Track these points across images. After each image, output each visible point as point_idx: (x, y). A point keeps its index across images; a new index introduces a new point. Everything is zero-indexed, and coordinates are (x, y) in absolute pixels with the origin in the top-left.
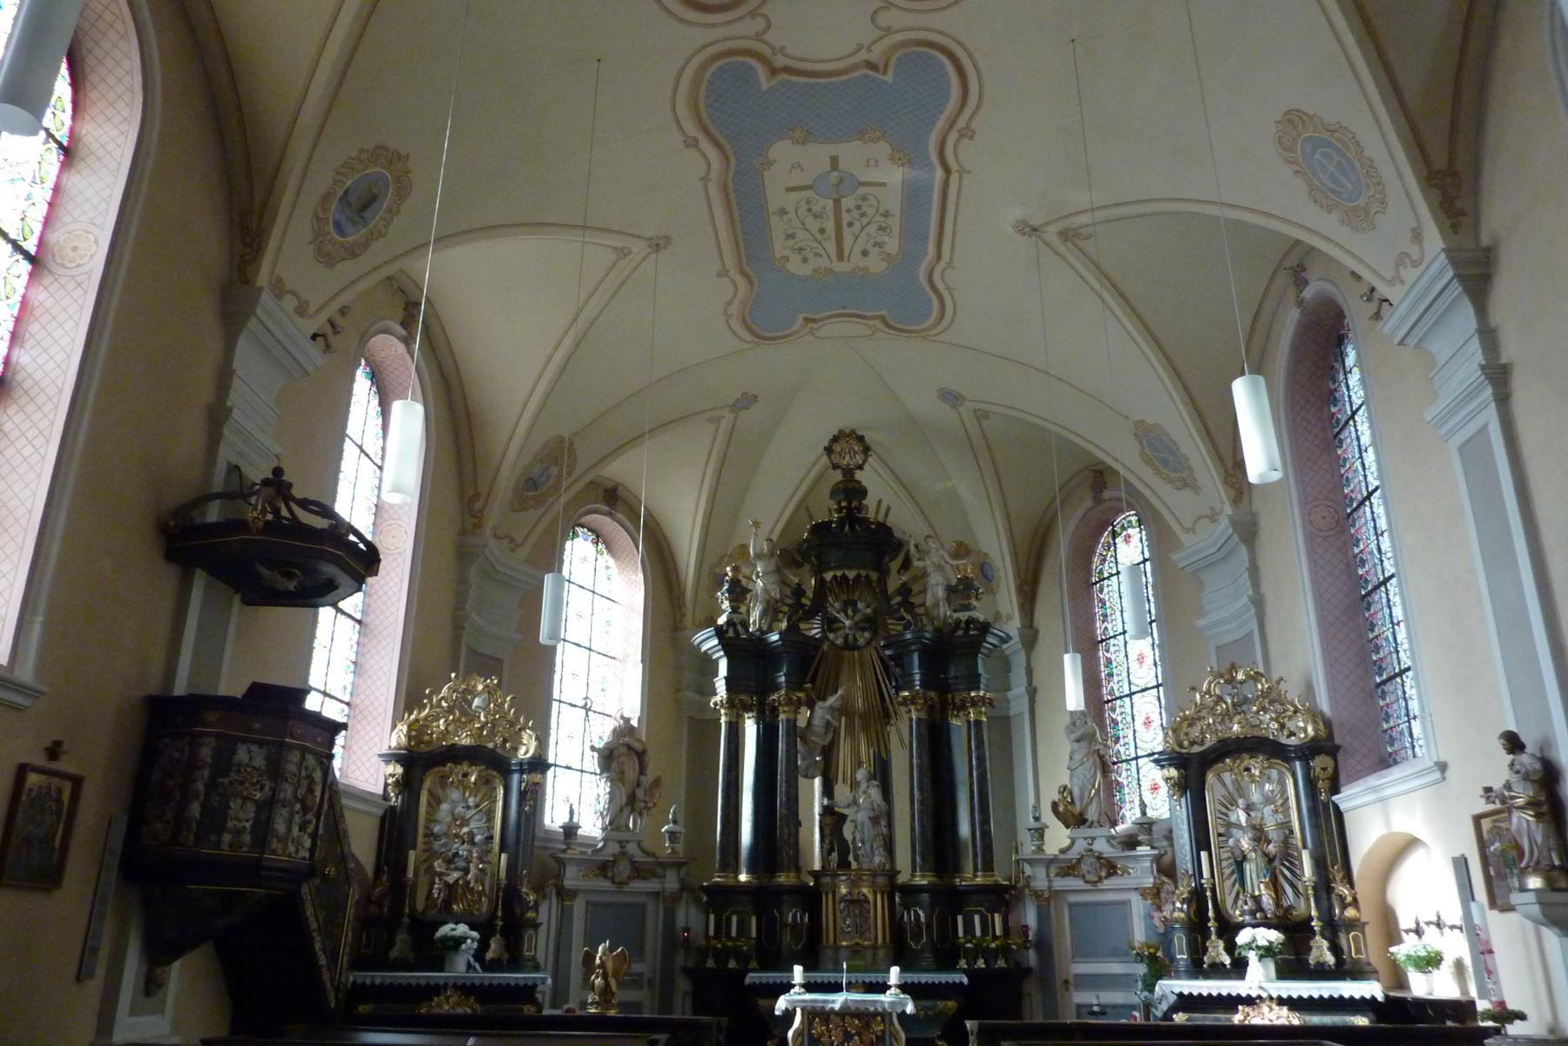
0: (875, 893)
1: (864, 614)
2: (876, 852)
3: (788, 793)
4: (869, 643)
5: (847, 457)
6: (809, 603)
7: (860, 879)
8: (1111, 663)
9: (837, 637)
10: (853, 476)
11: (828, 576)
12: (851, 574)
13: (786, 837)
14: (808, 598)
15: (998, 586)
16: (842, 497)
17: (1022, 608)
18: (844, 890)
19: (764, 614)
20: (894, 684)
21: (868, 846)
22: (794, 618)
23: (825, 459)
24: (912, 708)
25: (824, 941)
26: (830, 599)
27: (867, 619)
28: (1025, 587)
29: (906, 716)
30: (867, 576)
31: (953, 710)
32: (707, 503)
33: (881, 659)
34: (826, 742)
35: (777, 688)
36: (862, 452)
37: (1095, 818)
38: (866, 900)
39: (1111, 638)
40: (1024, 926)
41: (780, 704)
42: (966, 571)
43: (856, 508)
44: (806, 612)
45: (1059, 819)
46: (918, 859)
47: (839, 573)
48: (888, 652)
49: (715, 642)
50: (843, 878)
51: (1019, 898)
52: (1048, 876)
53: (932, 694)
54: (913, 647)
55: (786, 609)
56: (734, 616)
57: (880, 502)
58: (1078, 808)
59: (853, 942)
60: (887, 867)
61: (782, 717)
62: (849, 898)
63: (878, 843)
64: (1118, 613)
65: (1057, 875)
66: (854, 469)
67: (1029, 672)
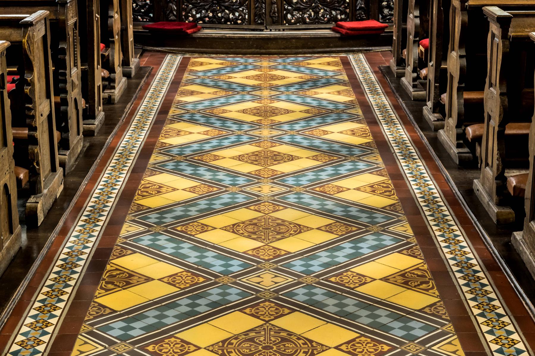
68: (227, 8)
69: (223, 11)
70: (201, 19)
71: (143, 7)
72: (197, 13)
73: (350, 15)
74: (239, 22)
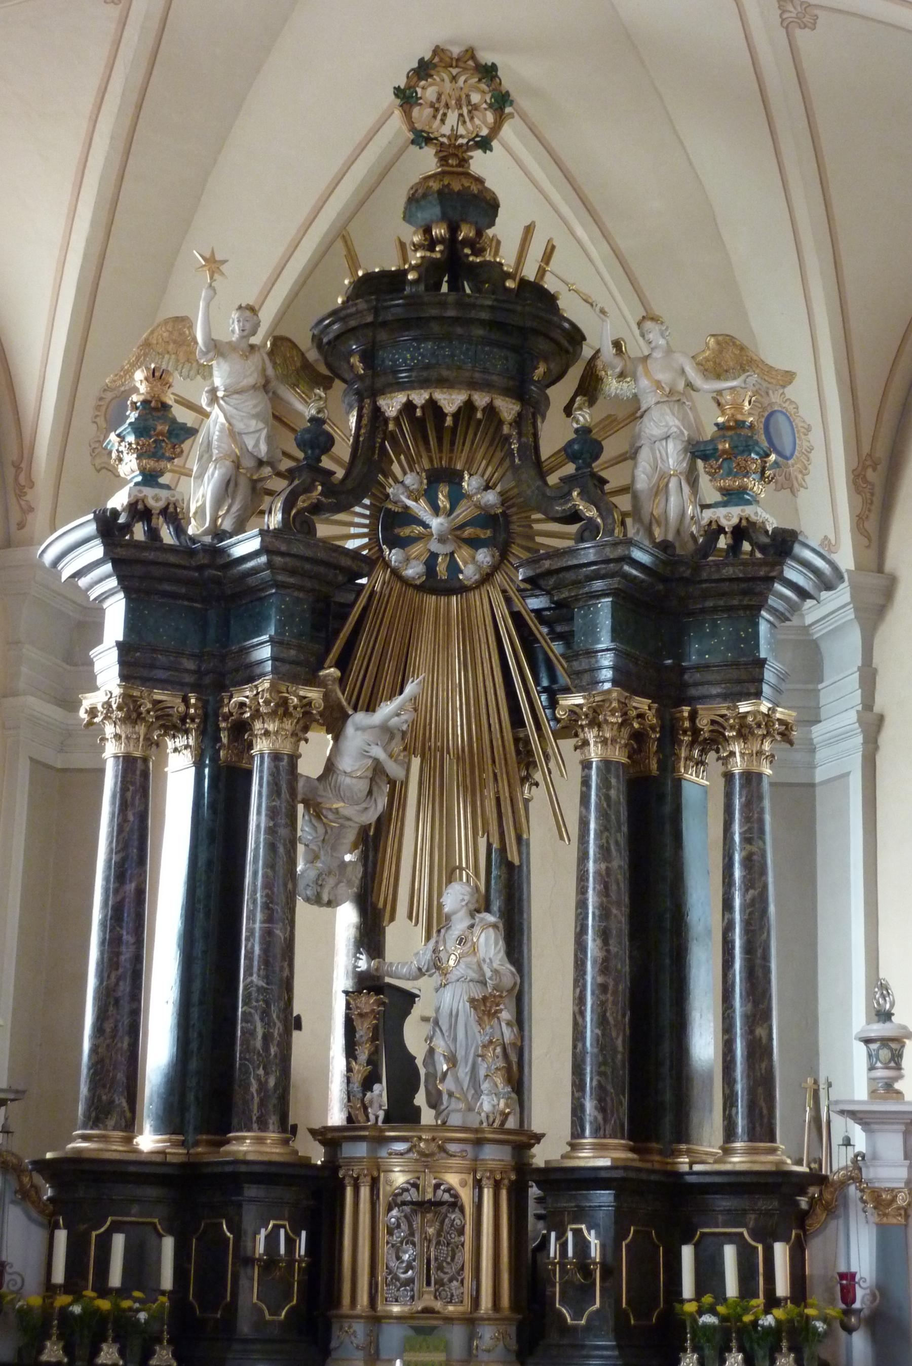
0: (478, 1185)
2: (485, 1086)
3: (268, 934)
4: (487, 578)
6: (340, 473)
7: (442, 1149)
9: (407, 560)
10: (464, 161)
11: (392, 404)
14: (337, 460)
15: (804, 471)
16: (437, 211)
17: (859, 522)
18: (399, 1179)
19: (227, 488)
20: (545, 683)
21: (463, 1072)
22: (301, 503)
23: (397, 120)
24: (591, 735)
25: (346, 1300)
26: (396, 468)
27: (487, 519)
29: (573, 758)
30: (491, 410)
31: (692, 745)
32: (94, 223)
33: (517, 618)
34: (371, 817)
35: (249, 674)
36: (491, 106)
38: (456, 1204)
41: (257, 714)
42: (738, 407)
43: (467, 242)
44: (331, 490)
46: (589, 1105)
47: (419, 397)
48: (535, 603)
49: (97, 550)
50: (400, 1147)
53: (642, 704)
54: (598, 585)
55: (279, 484)
56: (149, 492)
57: (529, 230)
60: (511, 1123)
61: (261, 746)
62: (413, 1195)
63: (492, 1062)
66: (468, 148)
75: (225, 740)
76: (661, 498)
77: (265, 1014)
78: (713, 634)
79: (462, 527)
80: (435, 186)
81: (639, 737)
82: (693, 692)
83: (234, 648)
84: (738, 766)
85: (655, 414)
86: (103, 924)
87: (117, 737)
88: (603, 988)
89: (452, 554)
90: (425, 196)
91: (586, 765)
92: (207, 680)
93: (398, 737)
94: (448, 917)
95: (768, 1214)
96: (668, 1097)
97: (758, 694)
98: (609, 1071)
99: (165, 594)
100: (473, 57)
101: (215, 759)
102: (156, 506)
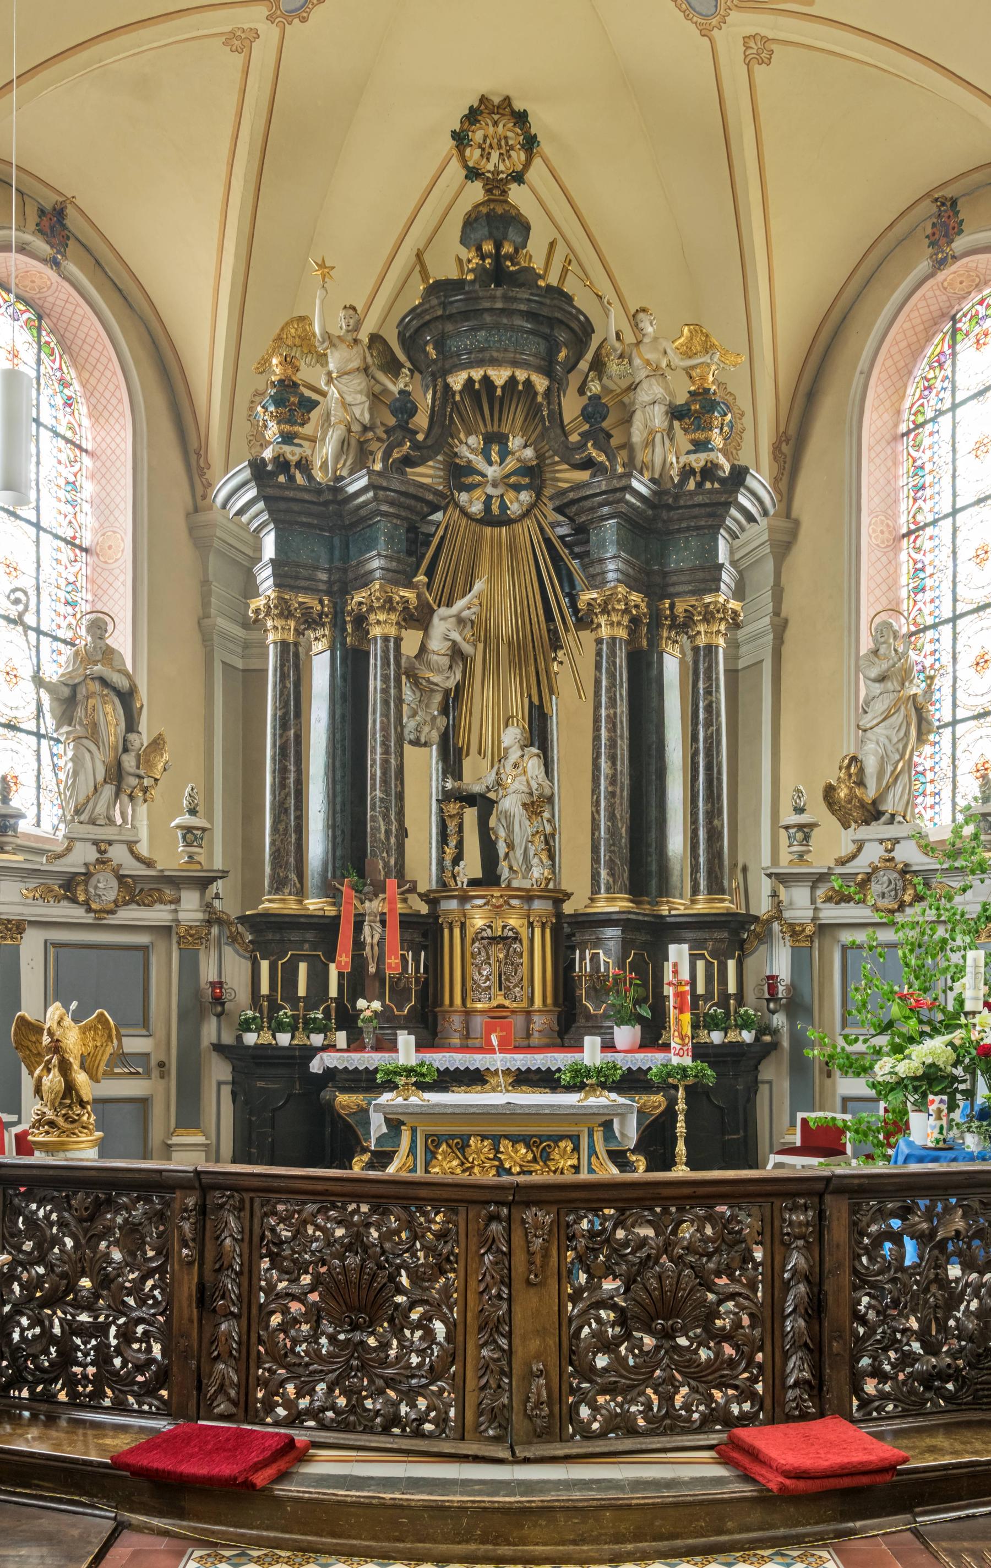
0: (531, 925)
1: (519, 460)
2: (535, 861)
3: (385, 763)
5: (495, 156)
8: (923, 569)
10: (504, 192)
12: (500, 376)
13: (383, 836)
16: (485, 231)
18: (479, 923)
21: (519, 852)
25: (447, 1001)
28: (785, 448)
31: (671, 628)
33: (548, 541)
35: (364, 581)
36: (523, 146)
37: (900, 809)
38: (517, 939)
39: (926, 525)
40: (769, 978)
43: (511, 258)
45: (833, 812)
46: (604, 873)
50: (480, 902)
51: (765, 937)
52: (813, 901)
53: (635, 597)
56: (287, 449)
58: (871, 793)
59: (495, 1003)
61: (376, 631)
63: (539, 842)
64: (947, 480)
65: (829, 900)
66: (506, 182)
67: (778, 593)
68: (390, 1382)
69: (381, 1392)
70: (311, 1413)
71: (140, 1368)
72: (300, 1395)
73: (768, 1403)
74: (428, 1427)
75: (350, 631)
76: (649, 450)
77: (386, 816)
78: (686, 549)
79: (508, 476)
80: (484, 210)
81: (635, 621)
82: (672, 590)
83: (354, 563)
84: (702, 641)
85: (645, 385)
86: (273, 758)
87: (275, 628)
88: (613, 794)
89: (502, 496)
90: (476, 219)
91: (599, 641)
92: (335, 588)
93: (469, 625)
94: (506, 749)
95: (721, 941)
96: (654, 867)
97: (718, 589)
98: (616, 849)
99: (303, 524)
100: (510, 105)
101: (343, 643)
102: (294, 459)
